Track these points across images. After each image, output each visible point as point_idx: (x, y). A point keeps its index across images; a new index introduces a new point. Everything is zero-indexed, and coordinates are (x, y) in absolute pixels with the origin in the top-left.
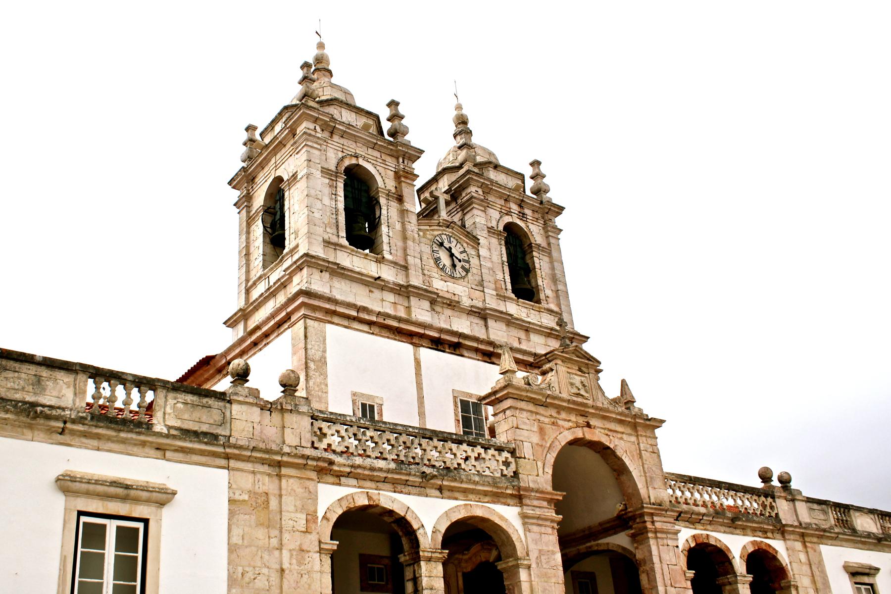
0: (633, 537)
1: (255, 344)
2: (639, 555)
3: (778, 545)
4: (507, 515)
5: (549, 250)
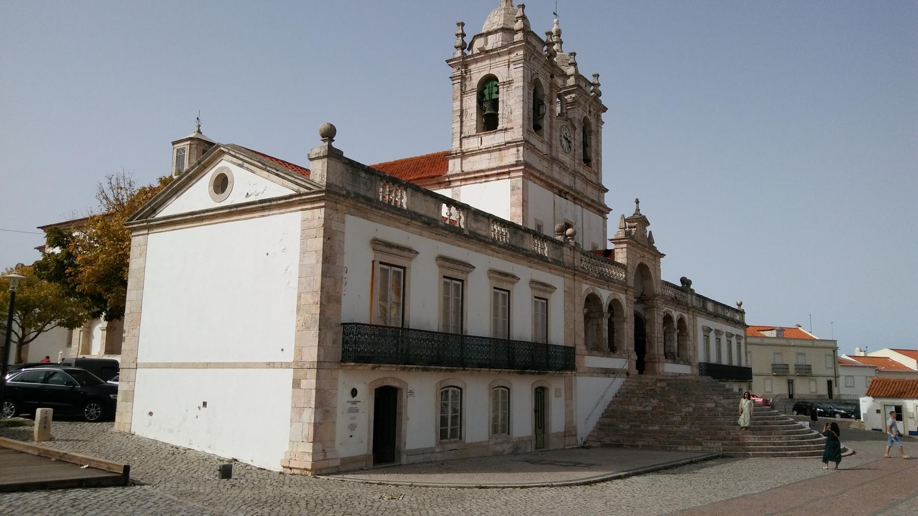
0: (645, 309)
1: (476, 178)
2: (647, 317)
3: (686, 316)
4: (622, 297)
5: (598, 133)
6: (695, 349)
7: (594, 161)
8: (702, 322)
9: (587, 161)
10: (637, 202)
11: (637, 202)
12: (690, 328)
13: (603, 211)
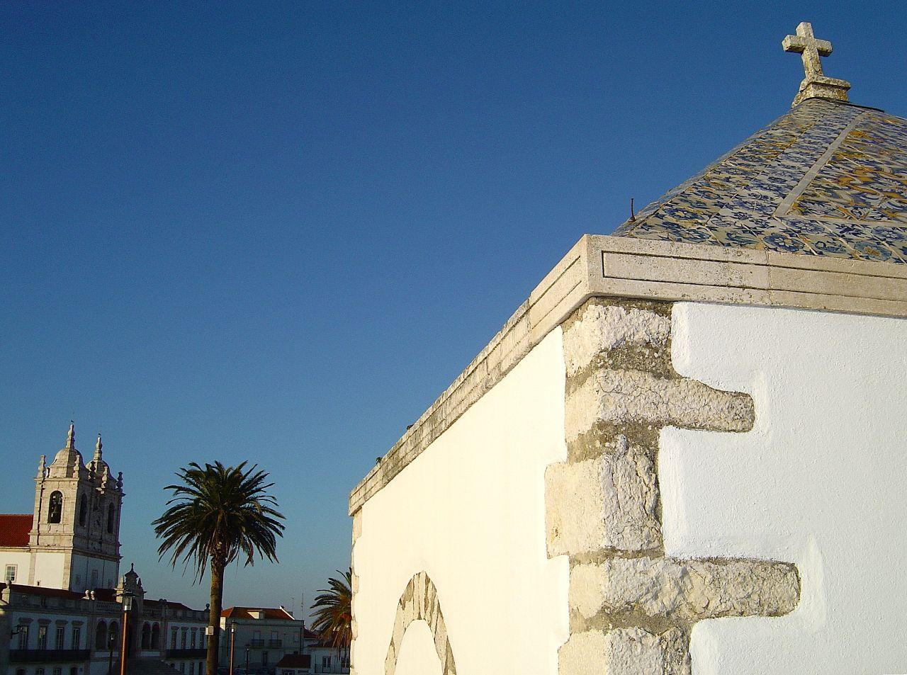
5: (119, 510)
6: (165, 641)
7: (114, 528)
8: (171, 624)
9: (110, 530)
10: (132, 564)
11: (132, 564)
12: (162, 631)
13: (117, 558)
